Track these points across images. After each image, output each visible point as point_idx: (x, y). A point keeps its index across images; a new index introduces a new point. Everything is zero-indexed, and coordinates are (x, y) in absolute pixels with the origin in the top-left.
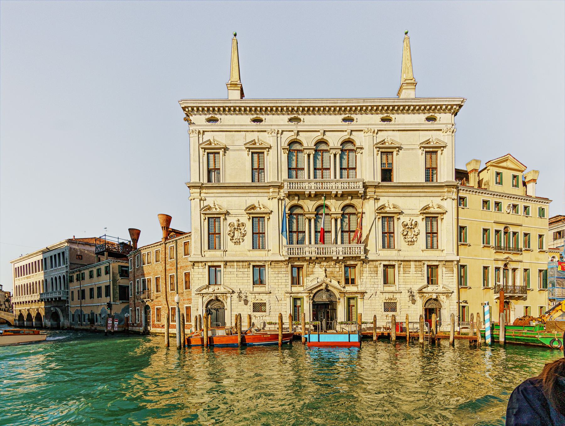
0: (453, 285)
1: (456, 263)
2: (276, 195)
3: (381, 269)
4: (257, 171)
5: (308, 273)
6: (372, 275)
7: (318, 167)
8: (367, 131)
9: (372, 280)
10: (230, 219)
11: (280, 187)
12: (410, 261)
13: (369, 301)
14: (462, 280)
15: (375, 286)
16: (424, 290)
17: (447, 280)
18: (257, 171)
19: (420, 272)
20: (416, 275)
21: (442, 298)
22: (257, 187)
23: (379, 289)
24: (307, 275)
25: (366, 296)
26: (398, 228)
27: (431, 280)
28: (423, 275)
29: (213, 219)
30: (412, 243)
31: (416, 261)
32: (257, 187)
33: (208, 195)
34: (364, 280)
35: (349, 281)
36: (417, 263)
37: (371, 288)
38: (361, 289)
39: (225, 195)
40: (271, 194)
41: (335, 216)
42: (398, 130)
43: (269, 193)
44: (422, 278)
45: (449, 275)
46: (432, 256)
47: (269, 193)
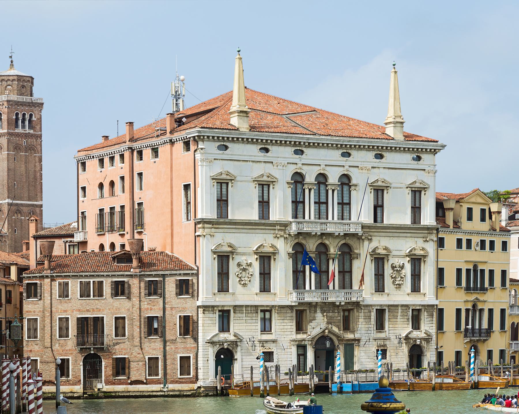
0: (433, 330)
1: (436, 307)
2: (282, 233)
3: (373, 314)
4: (264, 204)
5: (311, 318)
6: (366, 320)
7: (324, 205)
8: (364, 170)
9: (367, 326)
10: (238, 259)
11: (285, 225)
12: (397, 306)
13: (364, 349)
14: (440, 326)
15: (369, 332)
16: (410, 336)
17: (428, 326)
18: (264, 204)
19: (406, 317)
20: (402, 320)
21: (424, 343)
22: (264, 224)
23: (372, 335)
24: (311, 321)
25: (362, 343)
26: (388, 271)
27: (416, 326)
28: (408, 319)
29: (223, 259)
30: (399, 286)
31: (402, 306)
32: (264, 224)
33: (217, 230)
34: (360, 326)
35: (347, 327)
36: (404, 308)
37: (366, 335)
38: (357, 336)
39: (234, 230)
40: (277, 232)
41: (333, 256)
42: (389, 168)
43: (275, 230)
44: (408, 323)
45: (429, 319)
46: (416, 300)
47: (275, 230)
